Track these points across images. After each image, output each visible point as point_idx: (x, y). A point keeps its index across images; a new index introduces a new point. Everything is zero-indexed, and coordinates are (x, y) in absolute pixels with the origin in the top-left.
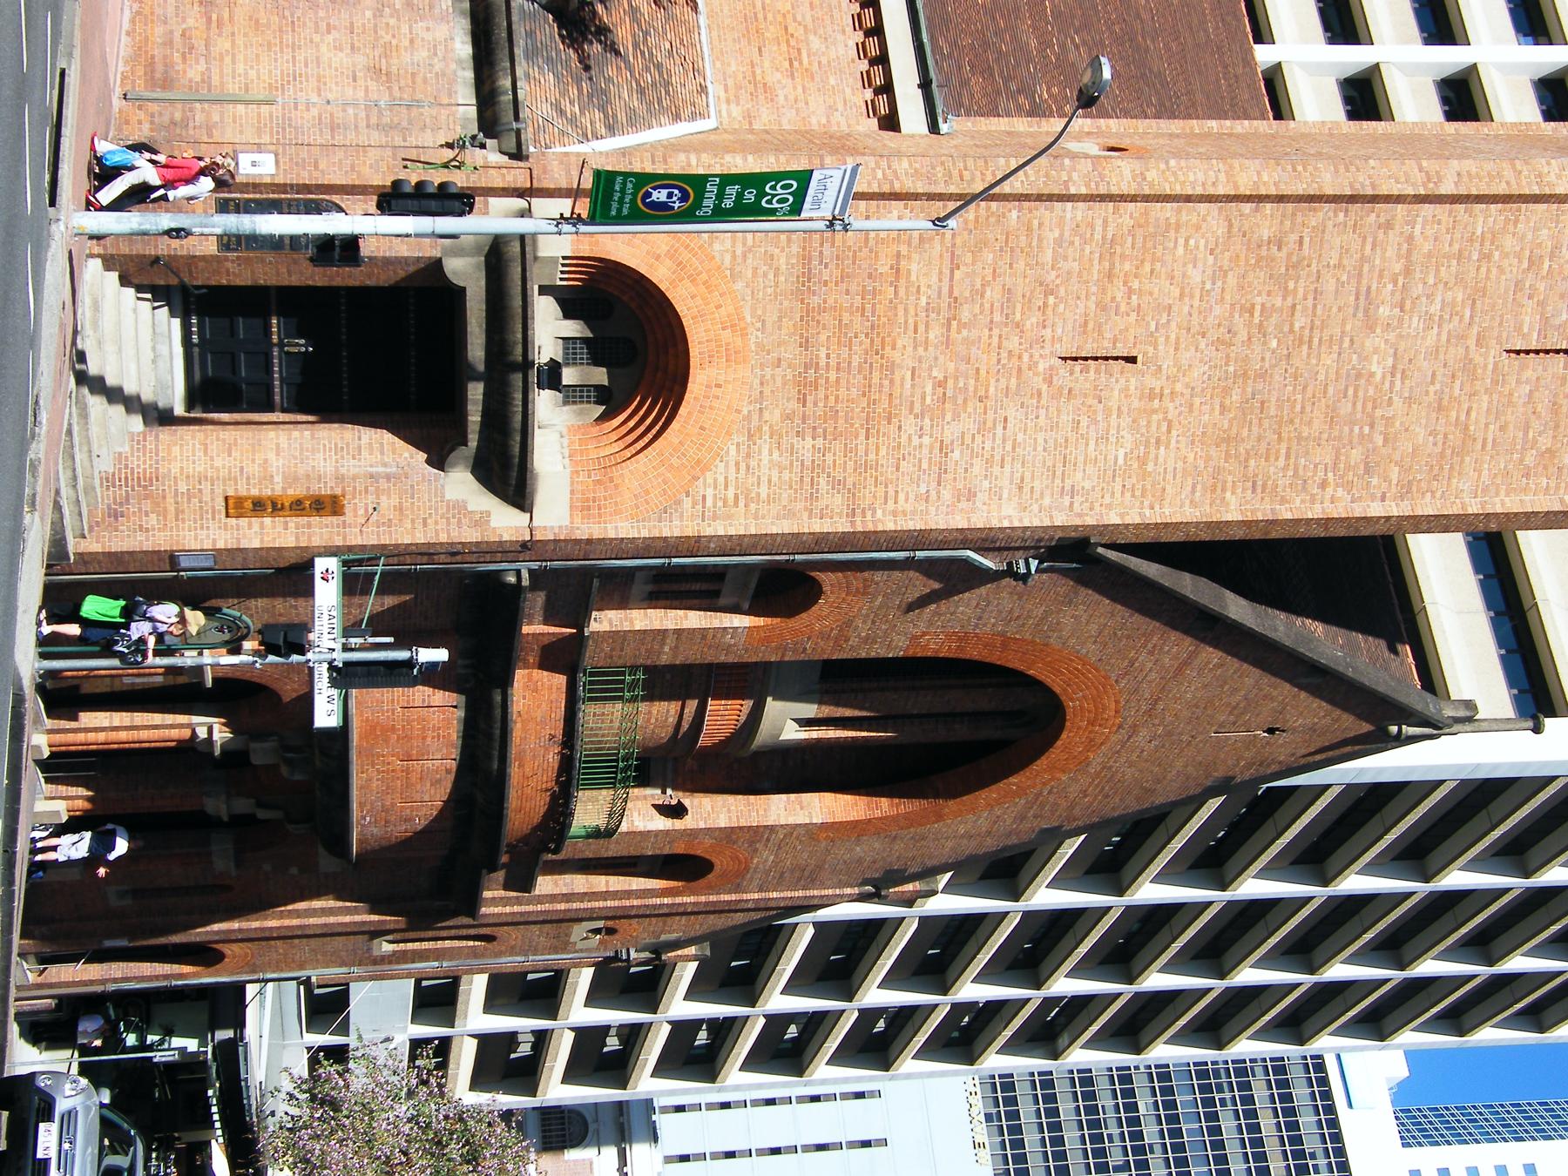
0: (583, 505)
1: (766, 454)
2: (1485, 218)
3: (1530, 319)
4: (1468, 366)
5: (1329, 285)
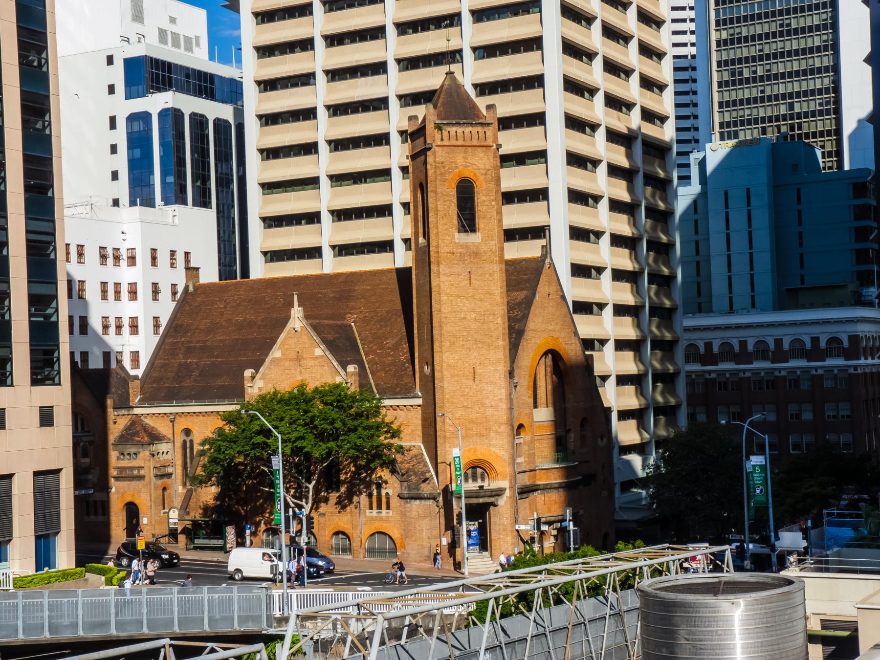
0: (504, 479)
1: (494, 442)
4: (473, 296)
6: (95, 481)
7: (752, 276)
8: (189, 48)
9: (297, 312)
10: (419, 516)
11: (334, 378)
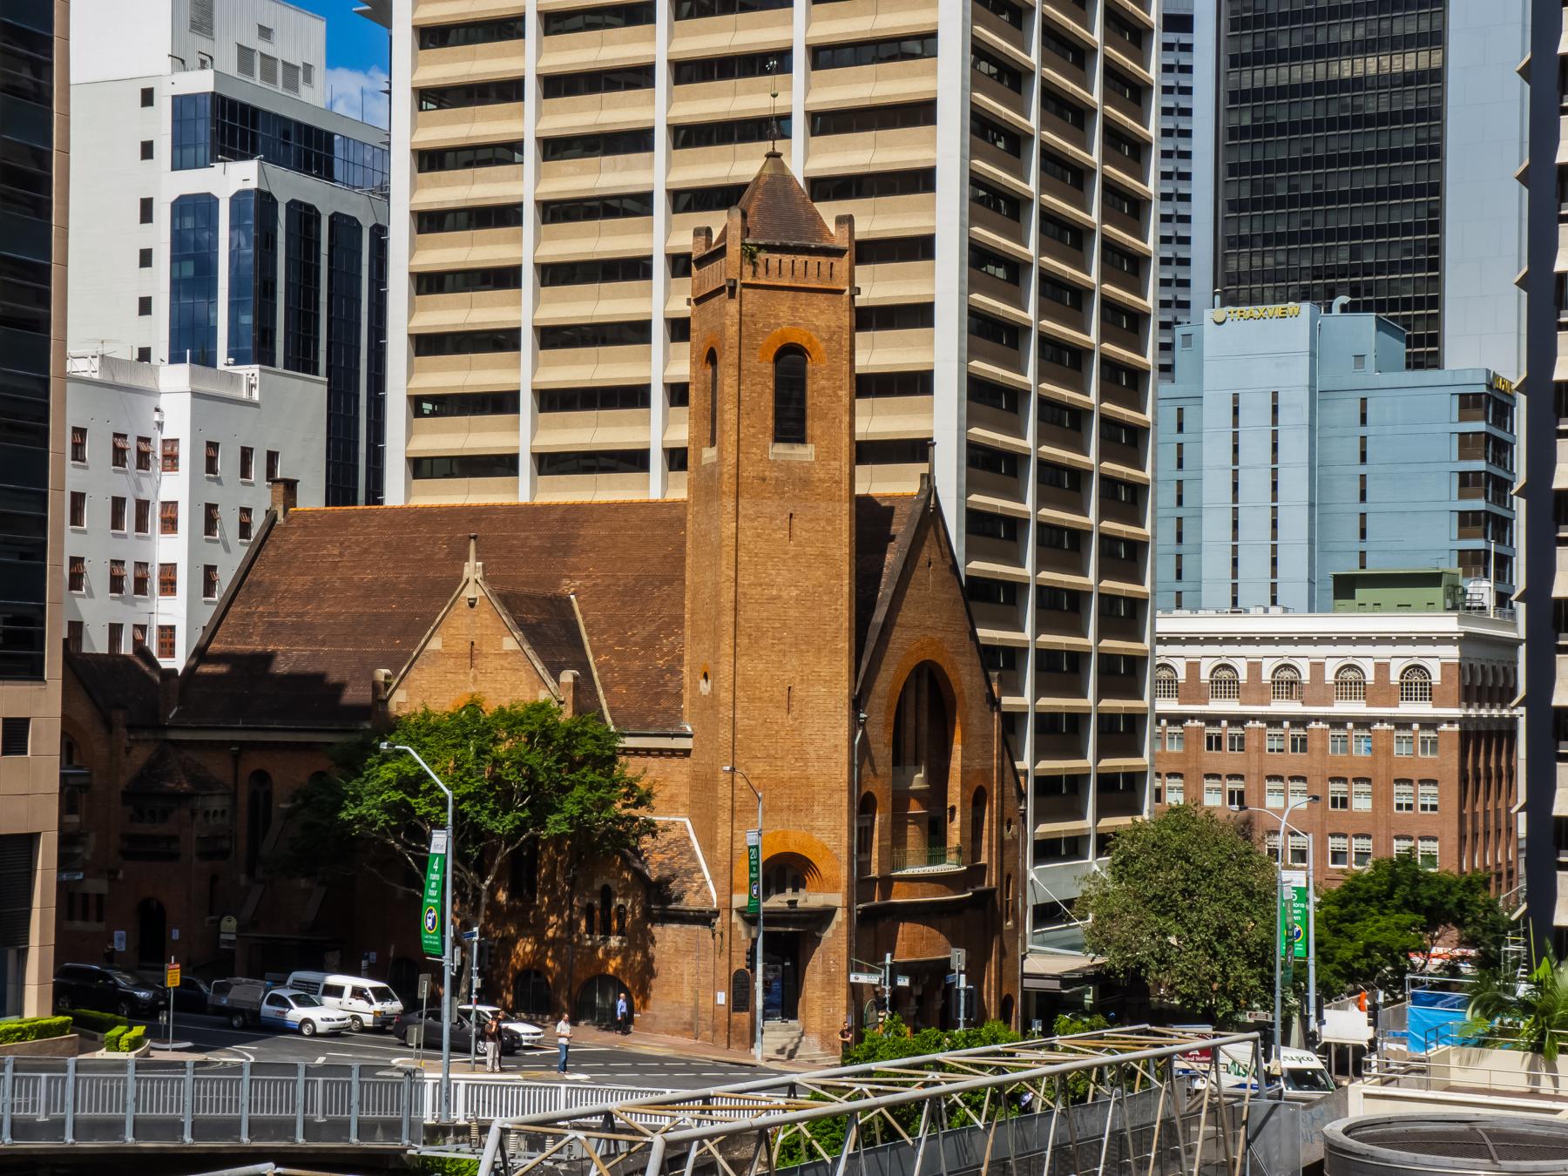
0: (835, 889)
1: (820, 823)
2: (743, 557)
3: (779, 535)
4: (795, 557)
5: (765, 615)
6: (88, 857)
7: (1274, 548)
8: (291, 85)
9: (472, 569)
10: (677, 950)
11: (536, 693)
